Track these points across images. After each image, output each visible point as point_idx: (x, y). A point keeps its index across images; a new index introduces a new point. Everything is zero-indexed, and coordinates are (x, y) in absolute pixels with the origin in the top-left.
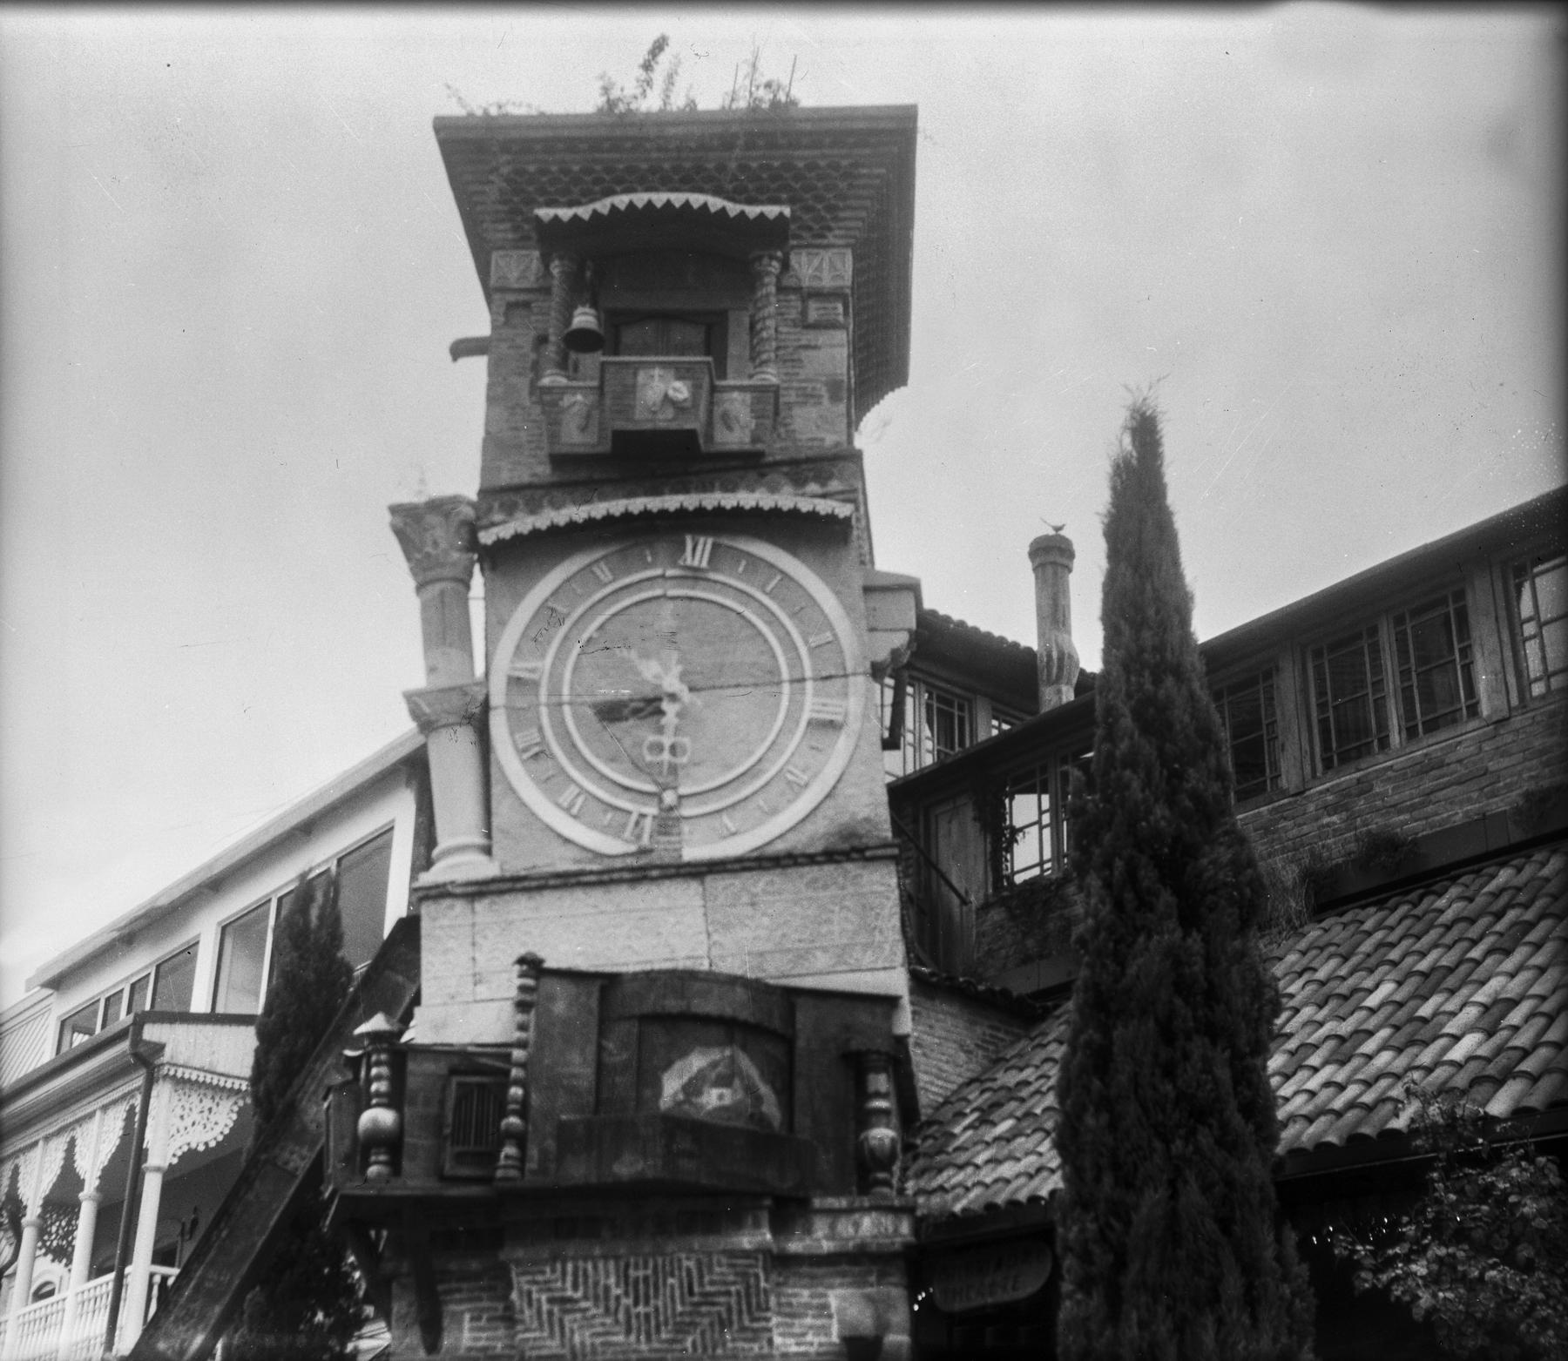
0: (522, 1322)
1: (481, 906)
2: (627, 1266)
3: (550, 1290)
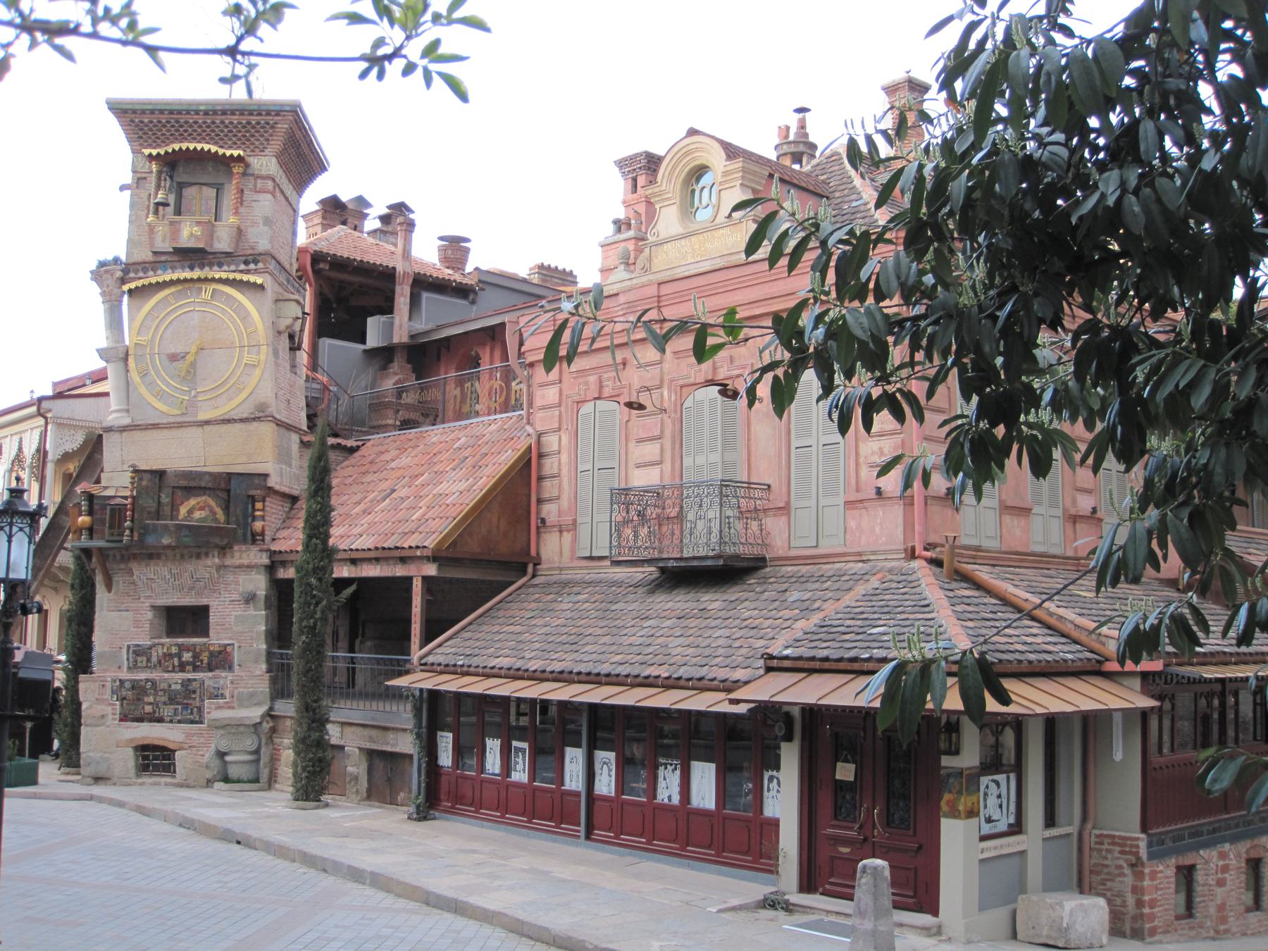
1: (125, 434)
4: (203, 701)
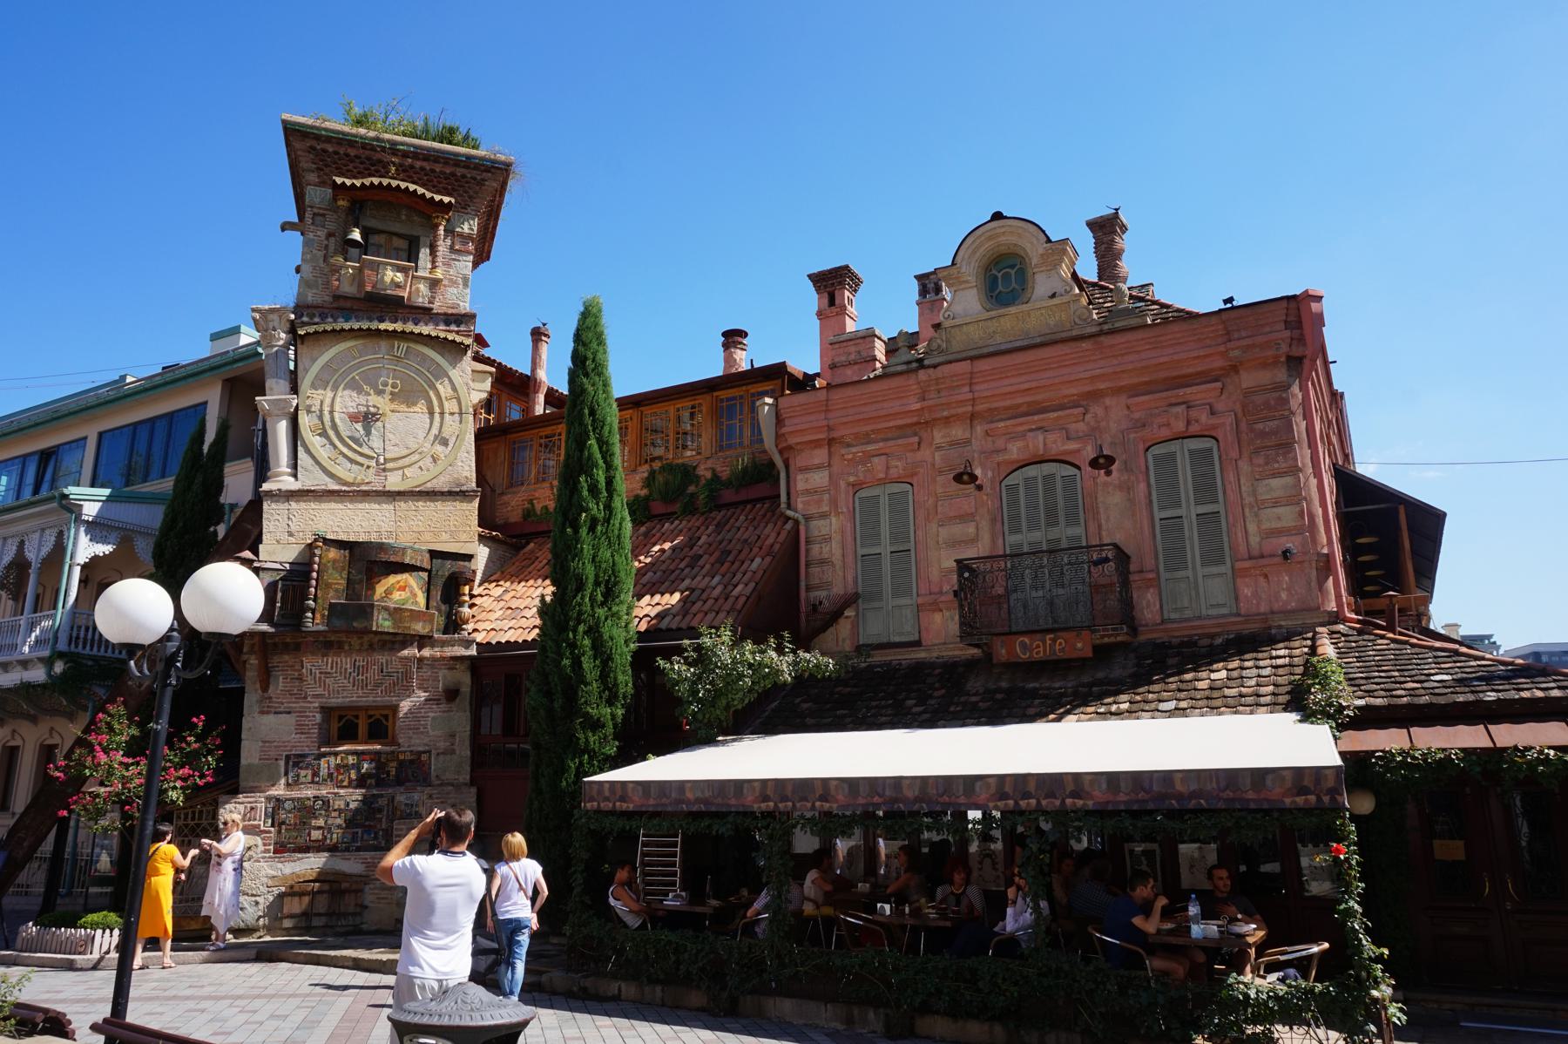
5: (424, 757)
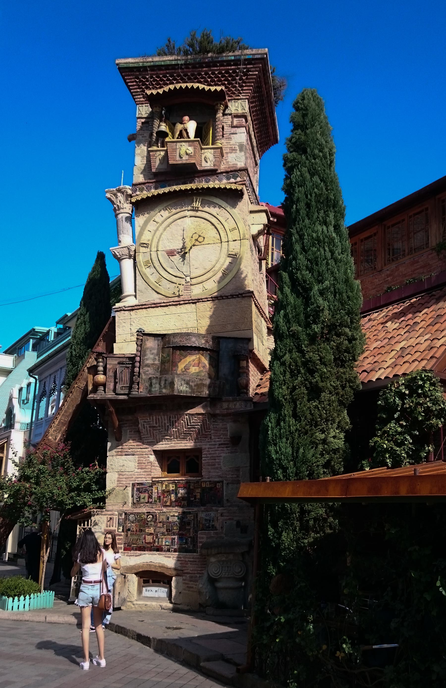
0: (143, 433)
2: (170, 417)
3: (149, 424)
4: (196, 532)
5: (219, 486)
